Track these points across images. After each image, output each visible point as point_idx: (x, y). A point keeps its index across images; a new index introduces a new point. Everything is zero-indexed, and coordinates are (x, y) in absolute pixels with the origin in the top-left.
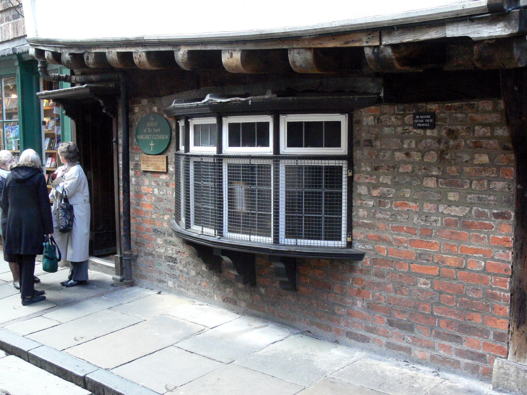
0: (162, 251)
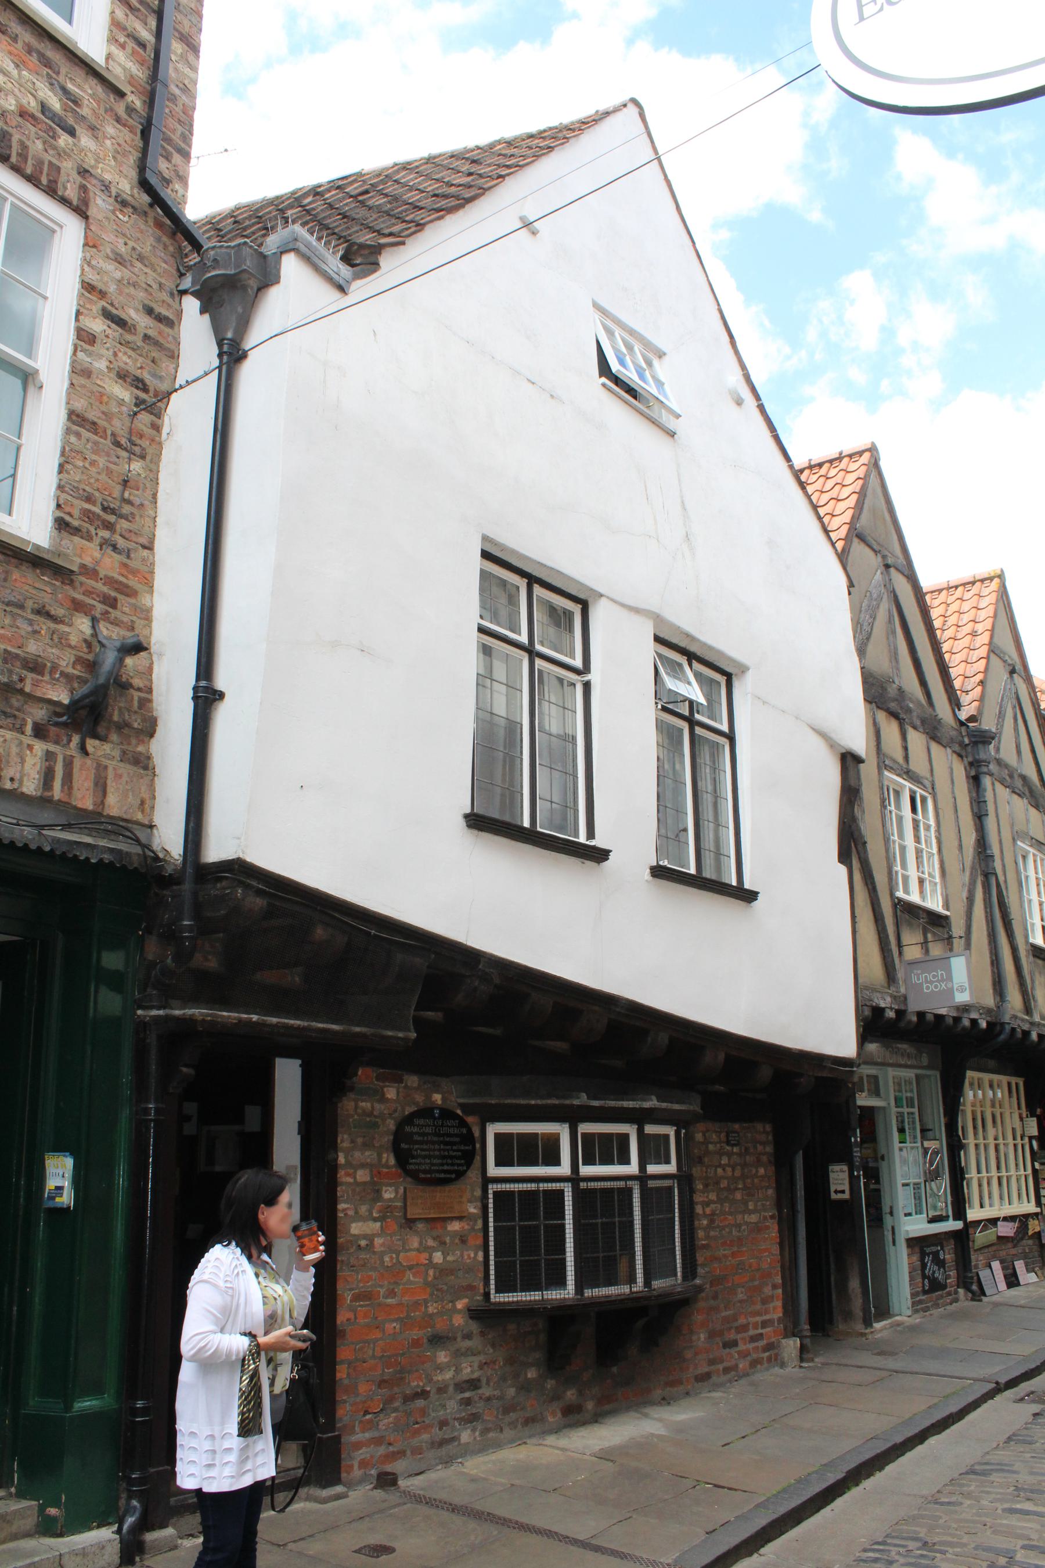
0: (449, 1375)
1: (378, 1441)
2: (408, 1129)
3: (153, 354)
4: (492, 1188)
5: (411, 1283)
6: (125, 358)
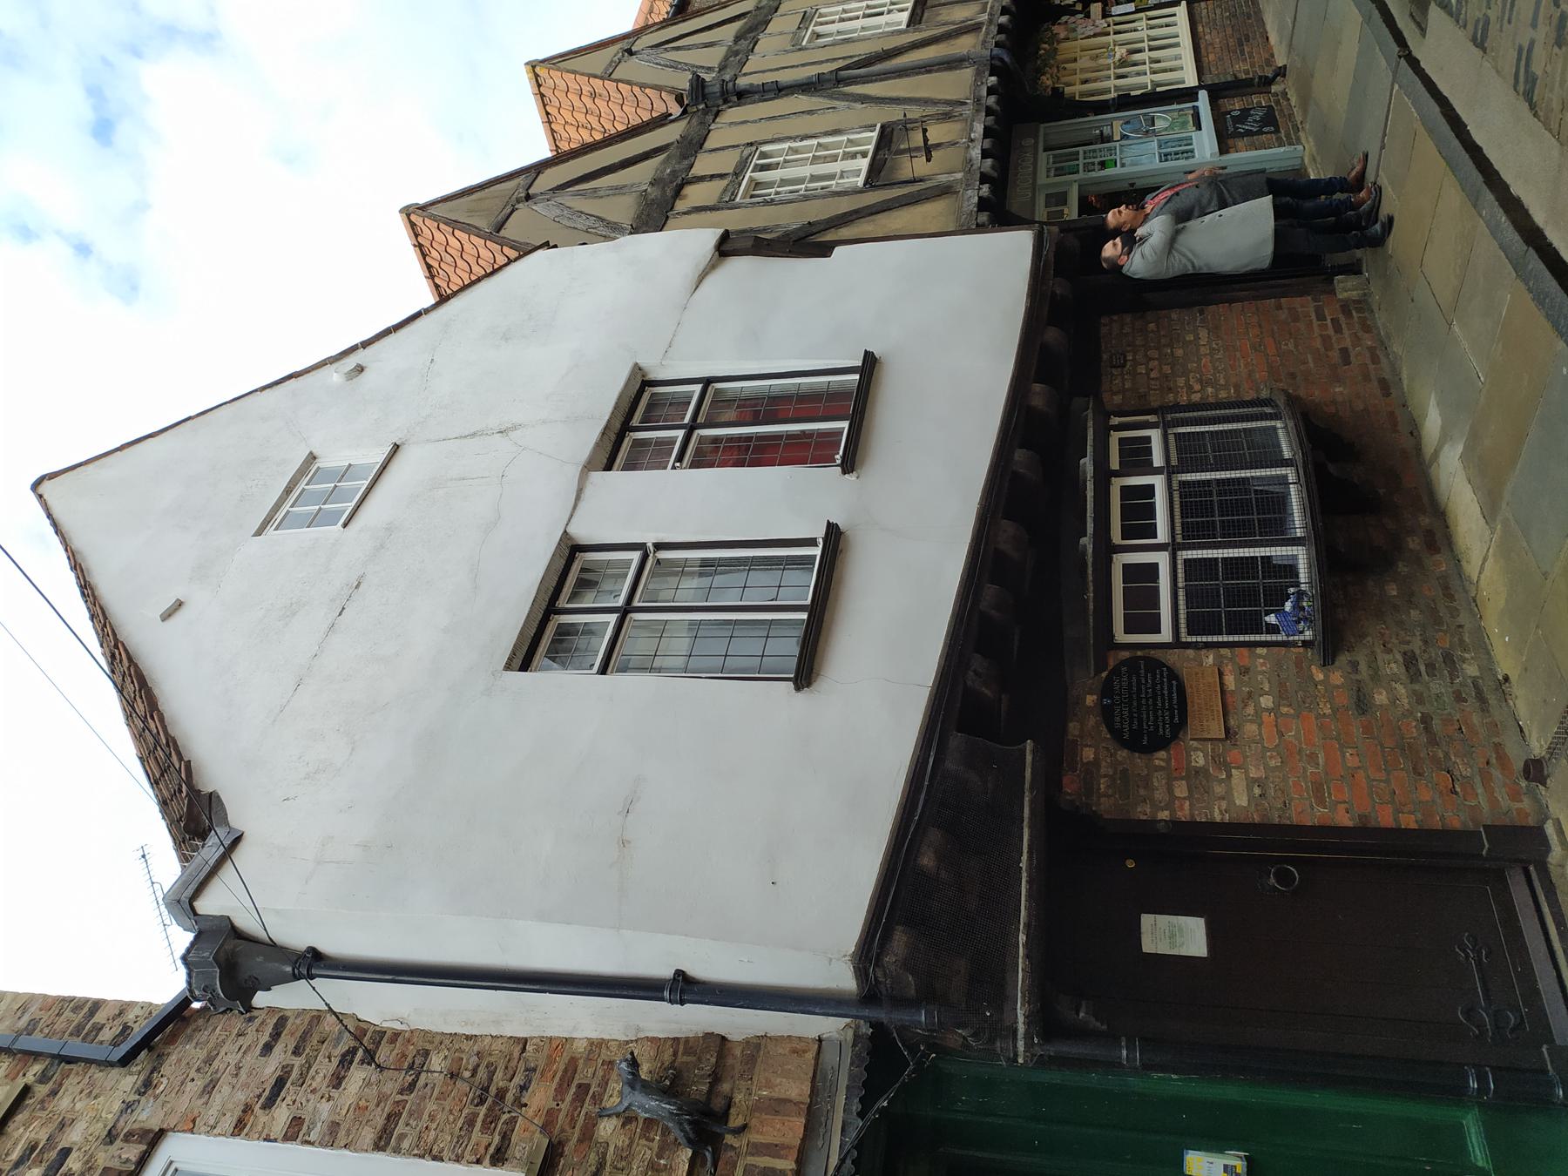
0: (1401, 690)
1: (1486, 779)
2: (1126, 736)
3: (315, 1042)
4: (1185, 638)
5: (1298, 732)
6: (319, 1079)
